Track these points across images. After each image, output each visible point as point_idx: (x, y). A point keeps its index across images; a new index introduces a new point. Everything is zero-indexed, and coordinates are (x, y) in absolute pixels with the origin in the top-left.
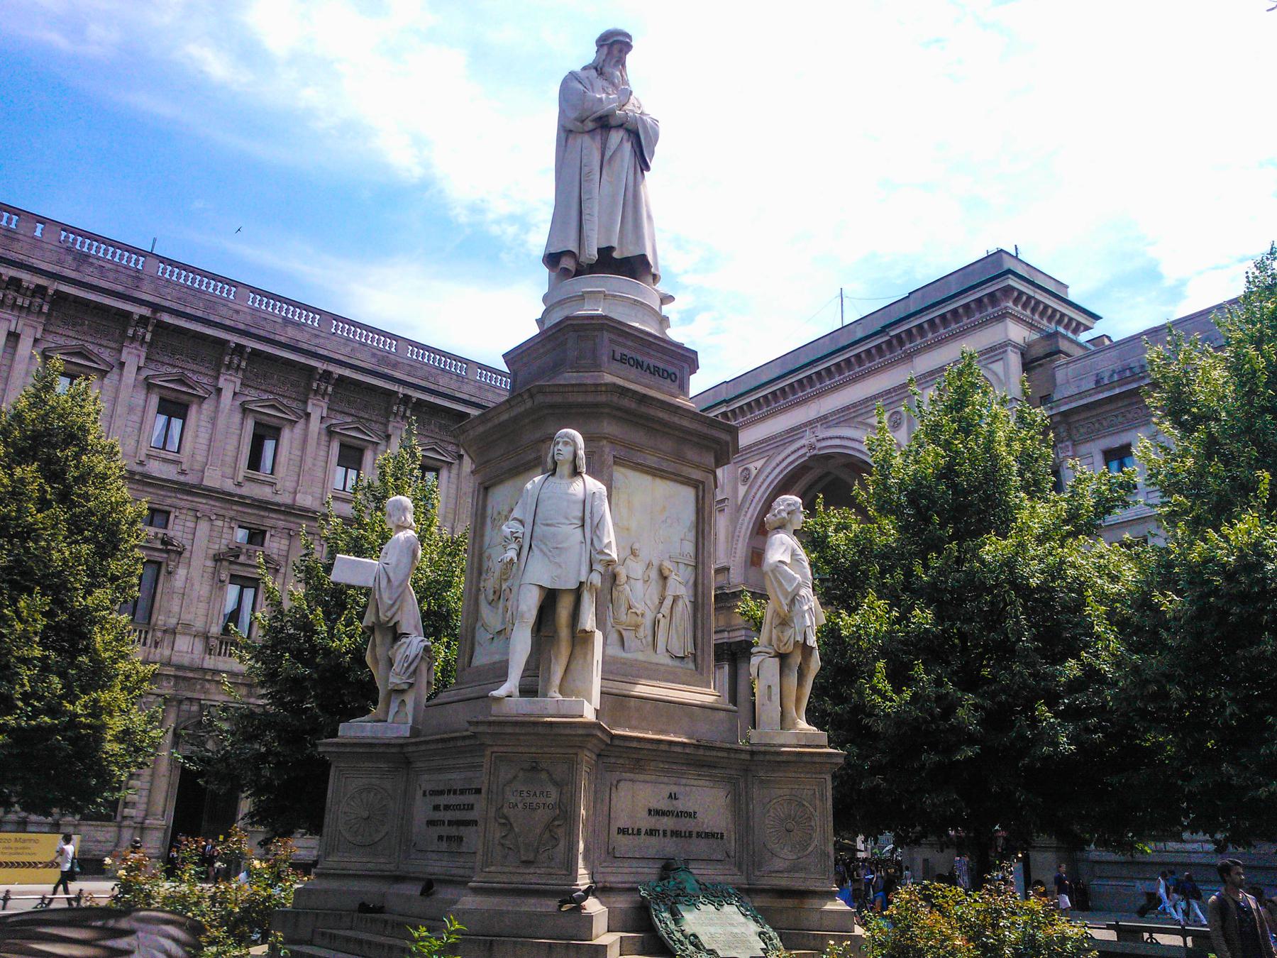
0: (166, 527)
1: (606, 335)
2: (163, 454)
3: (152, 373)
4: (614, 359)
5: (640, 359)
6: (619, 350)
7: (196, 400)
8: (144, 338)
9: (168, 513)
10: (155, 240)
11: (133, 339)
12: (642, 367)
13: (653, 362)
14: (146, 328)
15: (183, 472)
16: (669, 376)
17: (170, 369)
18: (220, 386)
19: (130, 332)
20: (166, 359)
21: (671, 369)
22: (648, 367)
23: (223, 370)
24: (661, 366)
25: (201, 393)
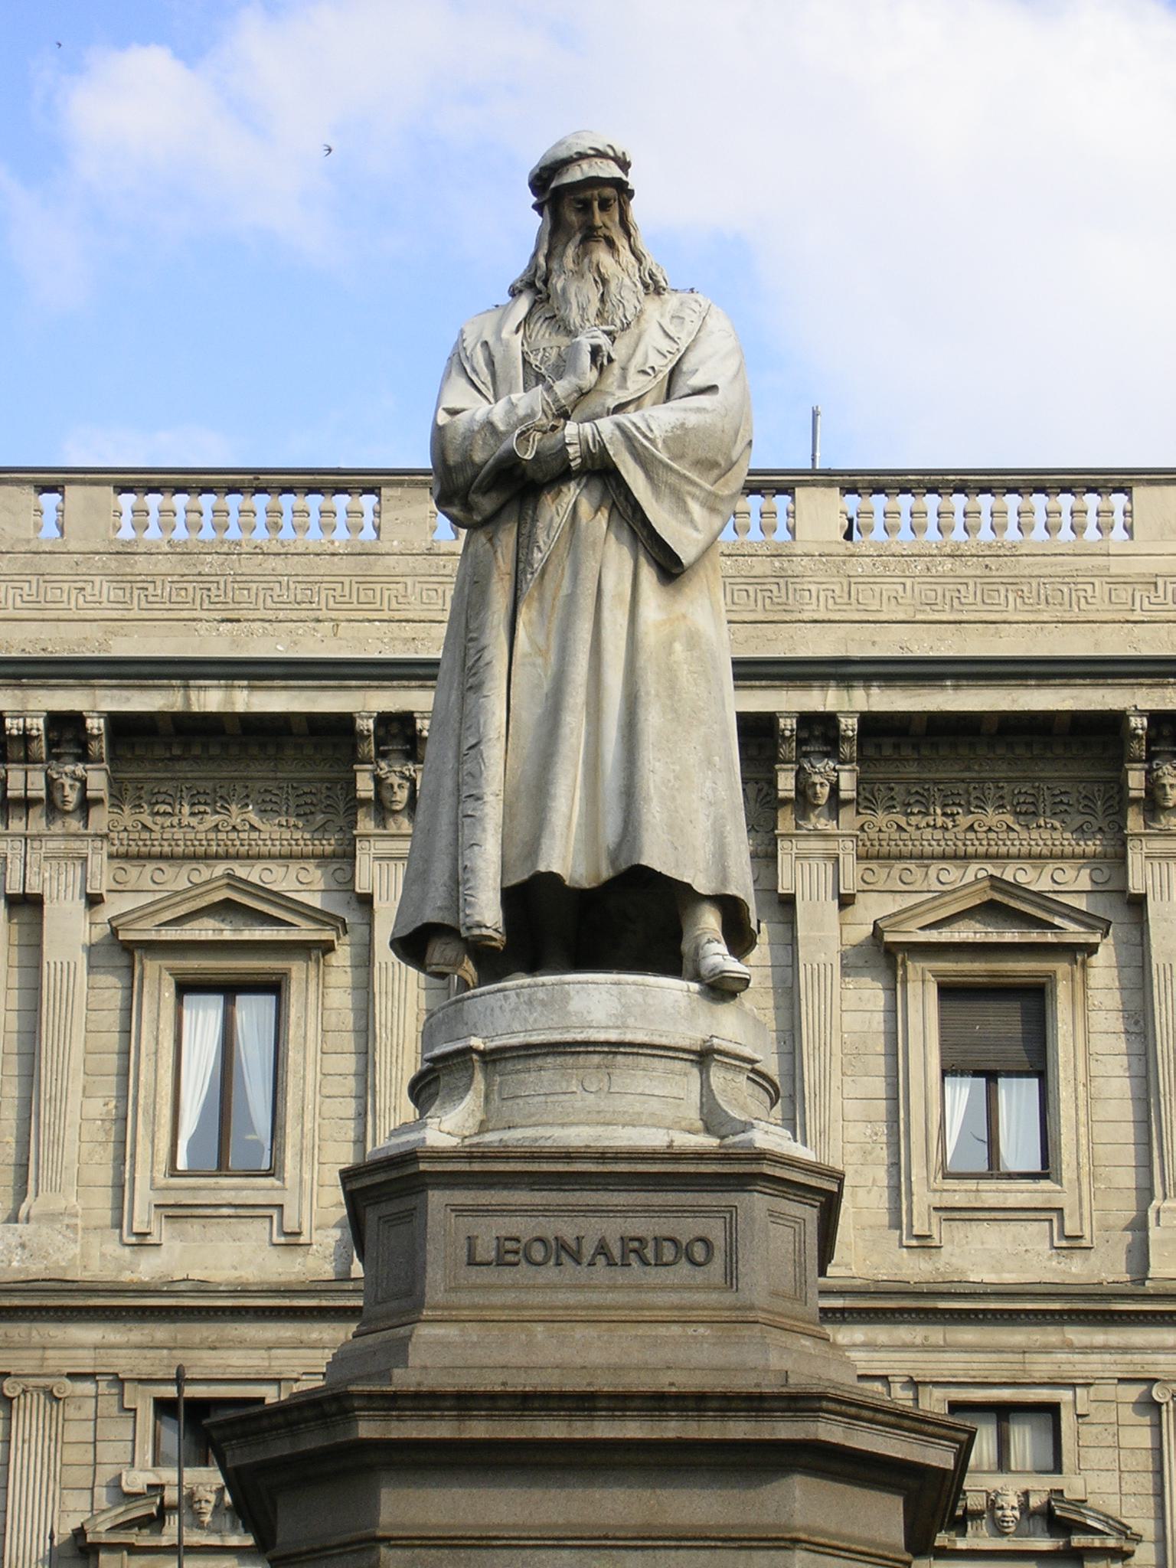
0: (1057, 1468)
1: (436, 1198)
2: (993, 1193)
3: (891, 905)
4: (472, 1262)
5: (566, 1229)
6: (489, 1232)
7: (1061, 968)
8: (835, 789)
9: (1052, 1410)
10: (815, 415)
11: (803, 802)
13: (613, 1229)
14: (833, 753)
15: (1073, 1244)
17: (953, 875)
18: (1135, 885)
19: (786, 783)
20: (931, 841)
21: (687, 1228)
22: (602, 1249)
23: (1134, 822)
25: (1074, 933)
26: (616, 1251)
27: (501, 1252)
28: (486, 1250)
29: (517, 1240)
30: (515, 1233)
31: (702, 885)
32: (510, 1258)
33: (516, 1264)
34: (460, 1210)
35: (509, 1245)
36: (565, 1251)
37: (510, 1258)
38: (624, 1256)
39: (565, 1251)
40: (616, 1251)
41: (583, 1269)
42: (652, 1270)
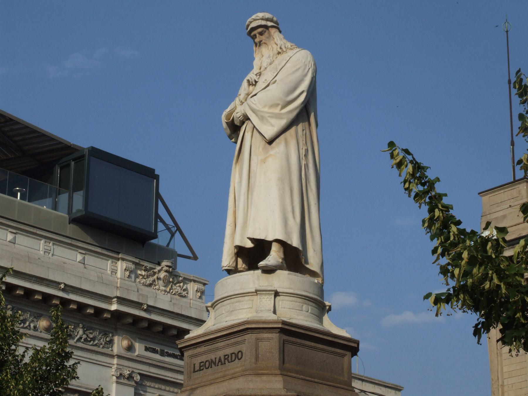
4: (194, 372)
5: (212, 356)
12: (215, 364)
13: (221, 354)
16: (237, 356)
21: (234, 349)
24: (228, 351)
26: (223, 360)
27: (200, 367)
28: (197, 368)
29: (203, 362)
30: (203, 360)
31: (270, 238)
32: (202, 368)
33: (203, 369)
34: (191, 357)
35: (202, 364)
36: (212, 363)
37: (202, 368)
38: (225, 361)
39: (212, 363)
40: (223, 360)
41: (216, 367)
42: (230, 364)
